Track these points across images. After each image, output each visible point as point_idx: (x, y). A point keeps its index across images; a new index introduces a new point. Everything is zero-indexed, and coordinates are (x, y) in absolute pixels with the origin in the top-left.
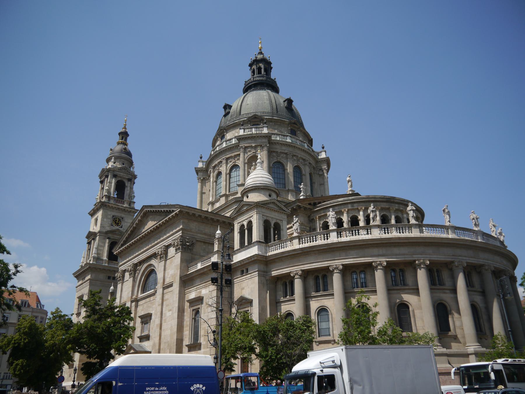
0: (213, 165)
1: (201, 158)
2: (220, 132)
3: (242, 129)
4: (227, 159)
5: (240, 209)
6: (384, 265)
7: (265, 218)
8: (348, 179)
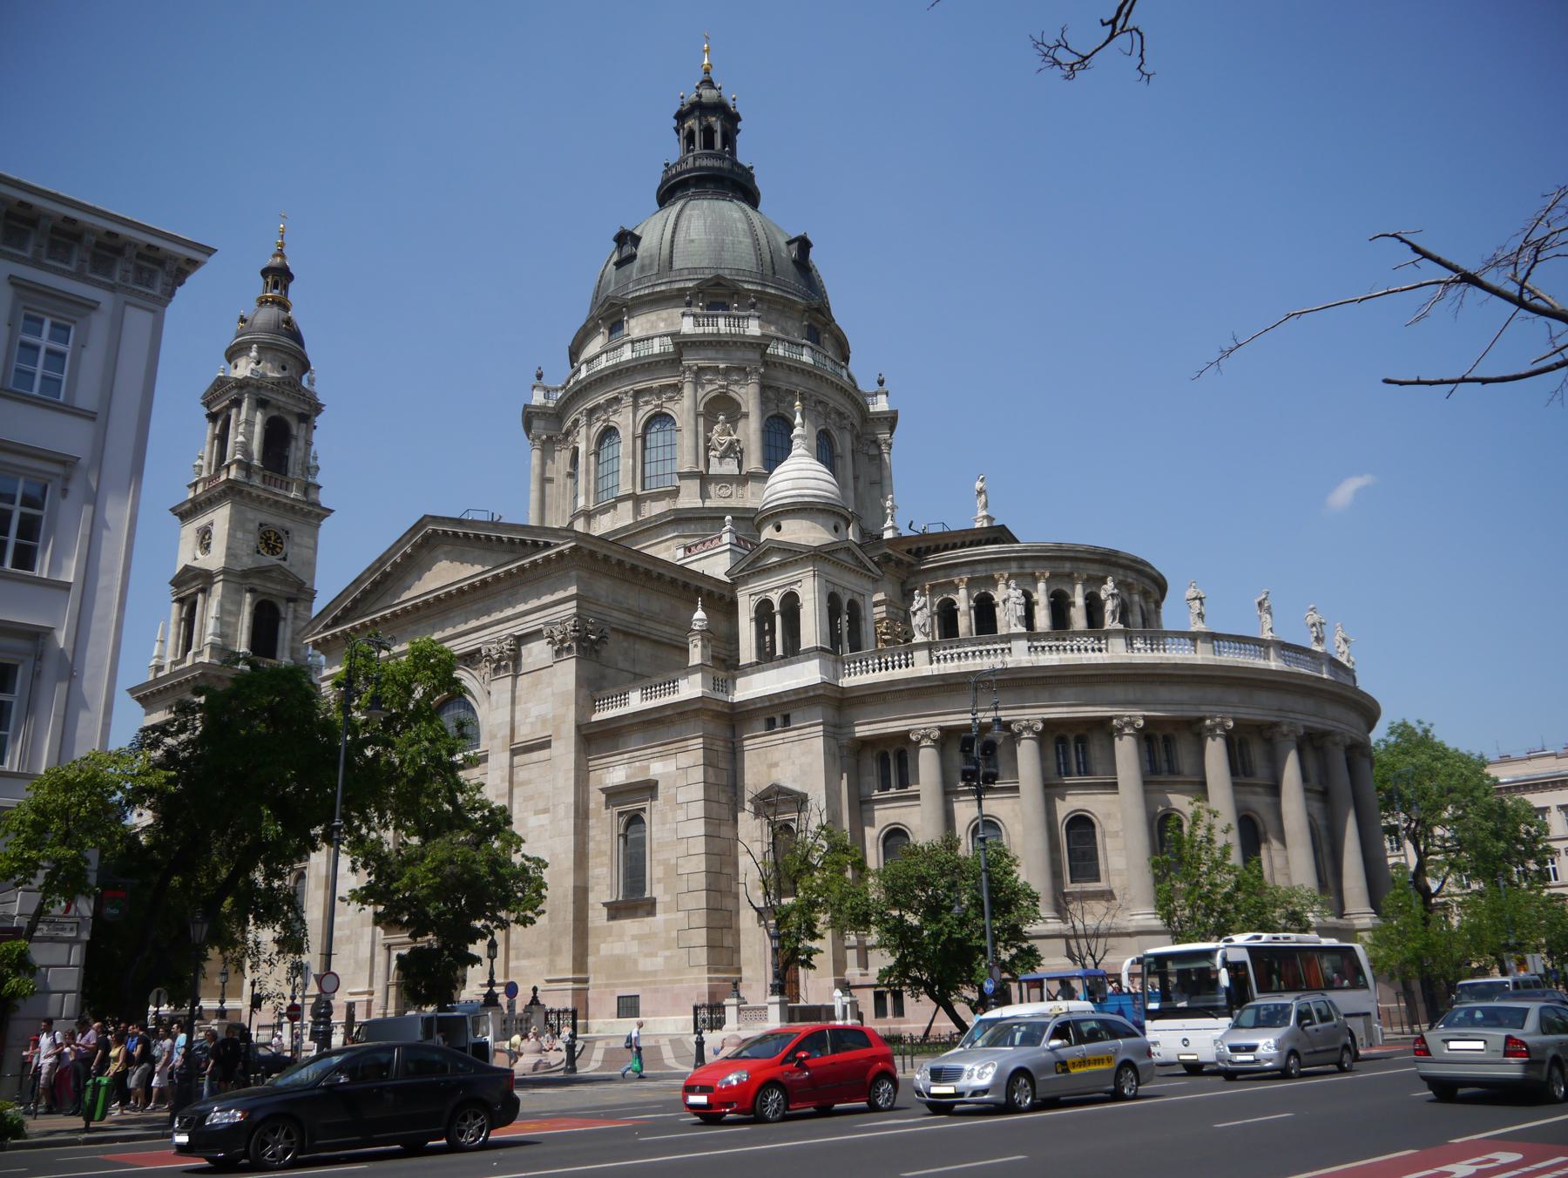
0: (589, 405)
1: (539, 376)
3: (689, 315)
4: (637, 394)
5: (758, 557)
7: (831, 588)
8: (978, 485)
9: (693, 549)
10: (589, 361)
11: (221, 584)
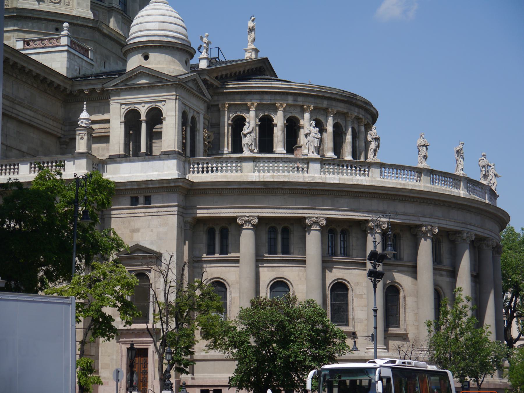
5: (131, 77)
6: (384, 227)
8: (250, 24)
9: (31, 43)
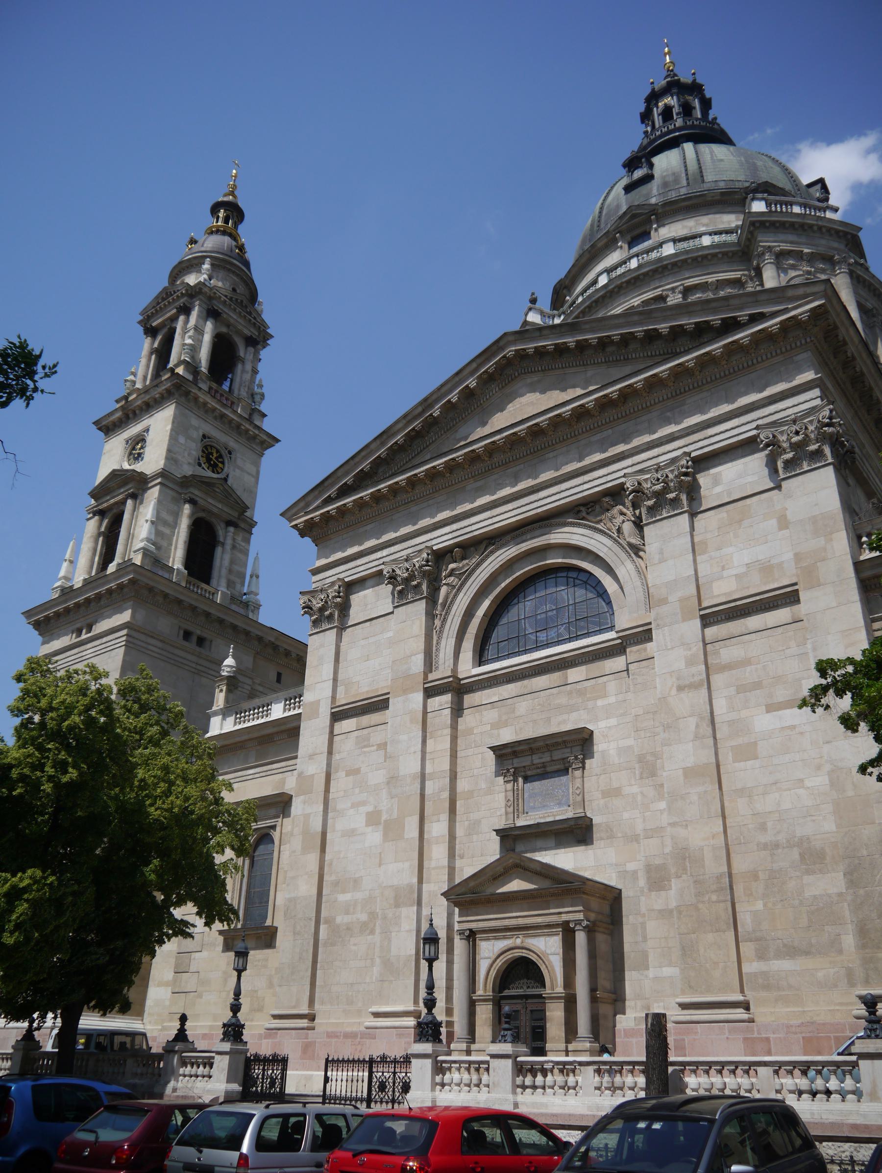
2: (626, 223)
10: (608, 271)
11: (158, 487)
